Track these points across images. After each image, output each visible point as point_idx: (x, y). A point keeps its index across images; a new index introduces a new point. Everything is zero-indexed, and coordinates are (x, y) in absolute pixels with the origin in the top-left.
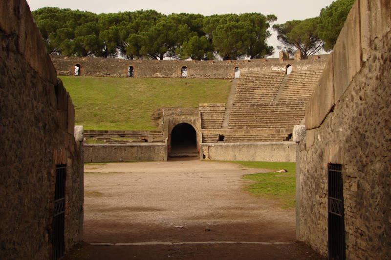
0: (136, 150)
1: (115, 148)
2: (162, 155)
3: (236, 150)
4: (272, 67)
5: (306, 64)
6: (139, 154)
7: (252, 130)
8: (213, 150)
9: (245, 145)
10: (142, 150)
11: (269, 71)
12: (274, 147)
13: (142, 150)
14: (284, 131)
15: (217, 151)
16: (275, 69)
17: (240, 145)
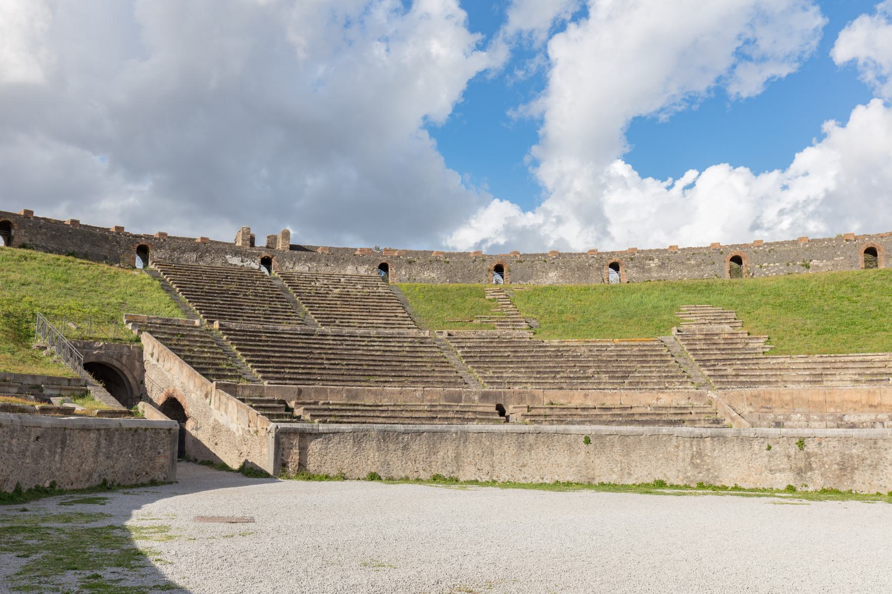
0: (94, 444)
1: (39, 432)
2: (162, 460)
3: (392, 447)
4: (227, 257)
5: (306, 261)
6: (101, 458)
7: (369, 391)
8: (314, 446)
9: (419, 433)
10: (111, 443)
11: (219, 263)
12: (531, 438)
13: (111, 443)
14: (476, 398)
15: (326, 448)
16: (235, 261)
17: (406, 433)
